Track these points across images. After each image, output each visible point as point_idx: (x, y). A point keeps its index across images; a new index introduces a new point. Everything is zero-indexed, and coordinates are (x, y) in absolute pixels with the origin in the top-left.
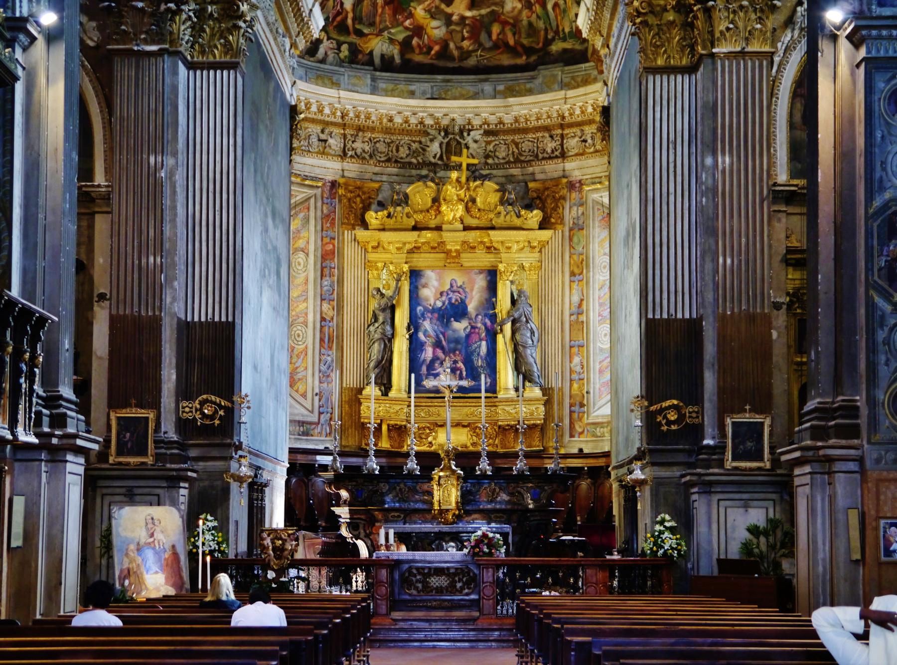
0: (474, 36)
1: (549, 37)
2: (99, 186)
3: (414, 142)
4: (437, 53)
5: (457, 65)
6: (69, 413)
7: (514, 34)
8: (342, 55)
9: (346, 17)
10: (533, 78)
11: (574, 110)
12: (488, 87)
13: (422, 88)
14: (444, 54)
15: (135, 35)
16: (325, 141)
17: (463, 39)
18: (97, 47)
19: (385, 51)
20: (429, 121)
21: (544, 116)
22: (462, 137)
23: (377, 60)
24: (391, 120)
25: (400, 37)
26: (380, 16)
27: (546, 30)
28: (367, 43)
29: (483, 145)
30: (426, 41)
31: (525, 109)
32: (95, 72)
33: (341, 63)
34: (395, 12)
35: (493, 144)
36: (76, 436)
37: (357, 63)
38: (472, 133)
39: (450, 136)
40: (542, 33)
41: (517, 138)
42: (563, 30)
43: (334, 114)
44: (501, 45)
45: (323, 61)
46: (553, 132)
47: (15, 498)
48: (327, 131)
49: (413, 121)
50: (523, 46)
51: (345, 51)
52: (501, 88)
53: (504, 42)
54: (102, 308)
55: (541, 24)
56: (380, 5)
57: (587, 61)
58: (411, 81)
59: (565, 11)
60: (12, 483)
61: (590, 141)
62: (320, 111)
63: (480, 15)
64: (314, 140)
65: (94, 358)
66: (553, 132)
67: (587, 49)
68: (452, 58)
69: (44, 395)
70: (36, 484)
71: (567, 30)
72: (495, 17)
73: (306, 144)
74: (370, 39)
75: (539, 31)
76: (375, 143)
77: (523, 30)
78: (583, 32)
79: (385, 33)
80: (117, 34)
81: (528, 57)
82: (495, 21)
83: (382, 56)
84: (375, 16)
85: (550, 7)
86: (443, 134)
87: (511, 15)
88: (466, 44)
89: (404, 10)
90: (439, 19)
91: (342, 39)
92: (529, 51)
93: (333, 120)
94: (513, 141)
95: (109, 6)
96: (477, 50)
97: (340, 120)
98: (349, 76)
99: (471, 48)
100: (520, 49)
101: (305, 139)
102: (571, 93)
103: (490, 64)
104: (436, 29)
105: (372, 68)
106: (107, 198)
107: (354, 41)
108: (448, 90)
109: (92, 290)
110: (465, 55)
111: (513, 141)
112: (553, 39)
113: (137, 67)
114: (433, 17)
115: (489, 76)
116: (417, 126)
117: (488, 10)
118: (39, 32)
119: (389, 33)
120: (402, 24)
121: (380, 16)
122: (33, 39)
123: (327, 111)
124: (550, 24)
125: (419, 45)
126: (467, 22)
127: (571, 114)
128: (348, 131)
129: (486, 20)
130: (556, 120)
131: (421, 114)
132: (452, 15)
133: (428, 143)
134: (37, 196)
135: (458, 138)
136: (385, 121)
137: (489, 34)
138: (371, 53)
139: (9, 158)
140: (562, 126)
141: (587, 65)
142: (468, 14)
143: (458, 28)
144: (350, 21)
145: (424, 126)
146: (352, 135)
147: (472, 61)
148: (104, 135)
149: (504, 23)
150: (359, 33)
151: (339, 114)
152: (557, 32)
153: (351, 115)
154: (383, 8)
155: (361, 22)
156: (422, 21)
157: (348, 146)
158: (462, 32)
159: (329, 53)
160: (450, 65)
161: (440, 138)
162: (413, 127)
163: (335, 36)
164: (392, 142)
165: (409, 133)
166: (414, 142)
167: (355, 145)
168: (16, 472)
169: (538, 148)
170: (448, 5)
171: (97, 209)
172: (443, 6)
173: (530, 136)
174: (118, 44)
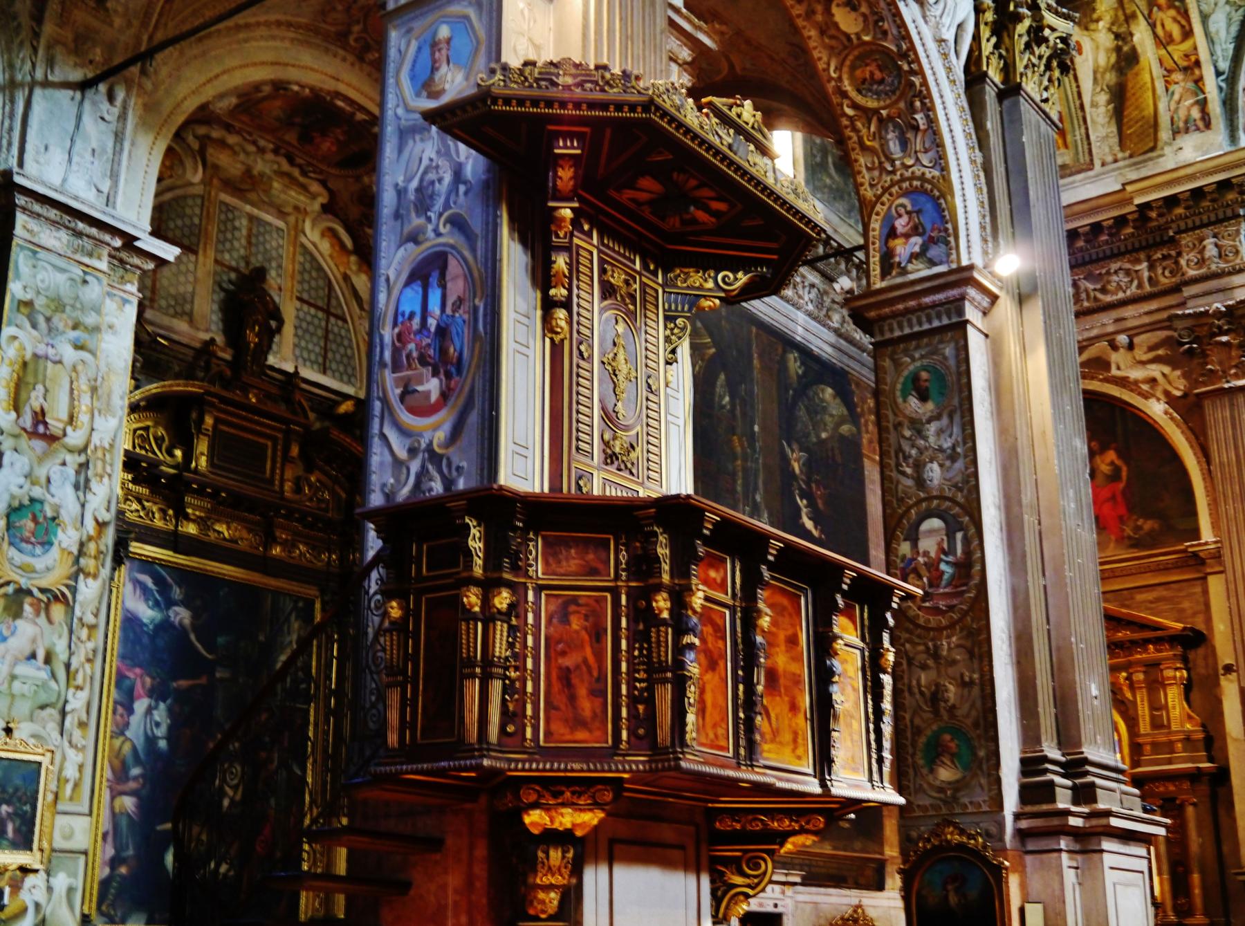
2: (1206, 543)
6: (1098, 781)
15: (1224, 372)
18: (1185, 395)
32: (1186, 422)
36: (1108, 814)
47: (1028, 907)
54: (1231, 681)
60: (1023, 886)
65: (1229, 741)
69: (1063, 759)
70: (1056, 886)
80: (1203, 375)
95: (1191, 348)
106: (1217, 556)
109: (1216, 663)
113: (1232, 405)
118: (1001, 288)
122: (994, 298)
134: (1019, 492)
139: (970, 444)
148: (1206, 487)
168: (1028, 870)
171: (1209, 570)
174: (1206, 386)
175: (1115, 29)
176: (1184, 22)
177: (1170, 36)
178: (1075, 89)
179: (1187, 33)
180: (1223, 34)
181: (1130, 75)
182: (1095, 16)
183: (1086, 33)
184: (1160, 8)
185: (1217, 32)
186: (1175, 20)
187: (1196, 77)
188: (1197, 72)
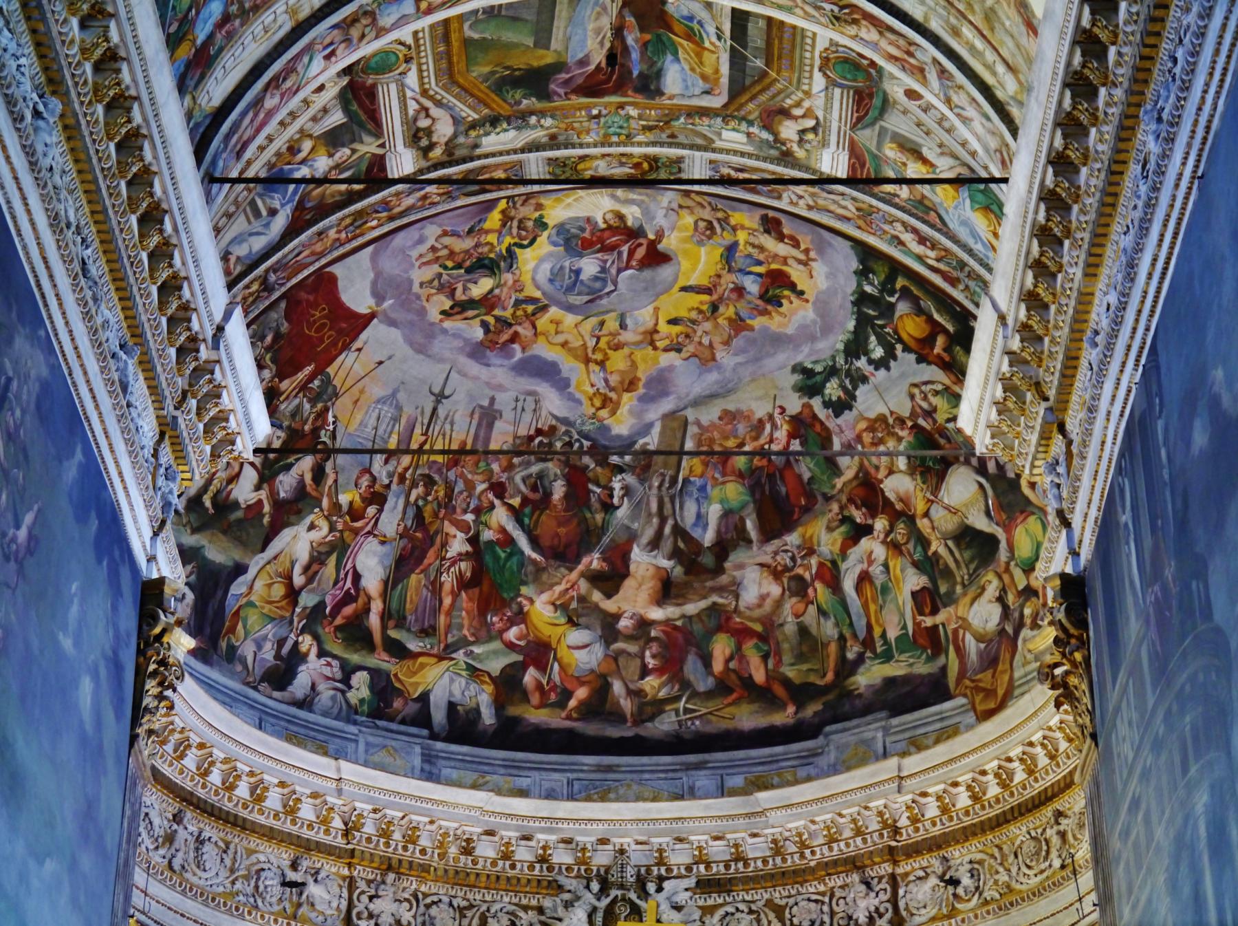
0: (671, 665)
1: (850, 655)
3: (526, 908)
4: (582, 703)
5: (630, 733)
7: (765, 658)
8: (353, 697)
9: (367, 610)
10: (815, 754)
11: (921, 807)
12: (703, 780)
13: (546, 785)
14: (599, 704)
16: (301, 885)
17: (645, 672)
19: (457, 697)
20: (562, 857)
21: (847, 833)
22: (645, 895)
23: (439, 716)
24: (467, 850)
25: (495, 666)
26: (449, 613)
27: (842, 639)
28: (415, 673)
29: (697, 915)
30: (556, 678)
31: (798, 817)
33: (350, 713)
34: (485, 607)
35: (721, 912)
37: (392, 720)
38: (666, 884)
39: (615, 892)
40: (833, 648)
41: (778, 895)
42: (884, 635)
43: (325, 821)
44: (734, 685)
45: (305, 704)
46: (870, 873)
48: (305, 864)
49: (523, 854)
50: (786, 682)
51: (361, 687)
52: (737, 781)
53: (740, 678)
55: (829, 629)
56: (447, 588)
57: (947, 696)
58: (513, 768)
59: (885, 590)
61: (966, 881)
62: (291, 811)
63: (683, 616)
64: (271, 882)
66: (870, 873)
67: (944, 669)
68: (617, 717)
71: (892, 634)
72: (719, 620)
73: (250, 890)
74: (423, 666)
75: (825, 645)
76: (428, 906)
77: (786, 646)
78: (977, 442)
79: (460, 655)
81: (800, 707)
82: (719, 629)
83: (452, 706)
84: (435, 612)
85: (848, 585)
86: (595, 886)
87: (757, 613)
88: (651, 684)
89: (505, 604)
90: (587, 627)
91: (355, 658)
92: (801, 693)
93: (321, 837)
94: (769, 903)
96: (677, 699)
97: (340, 841)
98: (367, 744)
99: (662, 694)
100: (779, 690)
101: (247, 878)
102: (913, 763)
103: (709, 729)
104: (580, 651)
105: (425, 732)
107: (385, 666)
108: (609, 790)
110: (650, 708)
111: (769, 903)
112: (860, 659)
114: (572, 622)
115: (706, 756)
116: (532, 868)
117: (703, 604)
119: (470, 654)
120: (501, 632)
121: (449, 613)
123: (307, 812)
124: (851, 625)
125: (539, 686)
126: (653, 634)
127: (914, 820)
128: (361, 872)
129: (697, 628)
130: (878, 841)
131: (540, 836)
132: (617, 617)
133: (561, 912)
135: (633, 896)
136: (453, 851)
137: (707, 660)
138: (424, 698)
140: (892, 854)
141: (947, 705)
142: (656, 614)
143: (632, 648)
144: (374, 620)
145: (550, 869)
146: (369, 882)
147: (665, 724)
149: (741, 634)
150: (398, 650)
151: (337, 823)
152: (868, 643)
153: (369, 829)
154: (455, 595)
155: (401, 623)
156: (547, 631)
157: (360, 907)
158: (643, 658)
159: (321, 687)
160: (614, 732)
161: (589, 898)
162: (522, 871)
163: (337, 649)
164: (471, 906)
165: (513, 885)
166: (526, 908)
167: (375, 906)
169: (832, 914)
170: (609, 596)
172: (597, 596)
173: (812, 888)
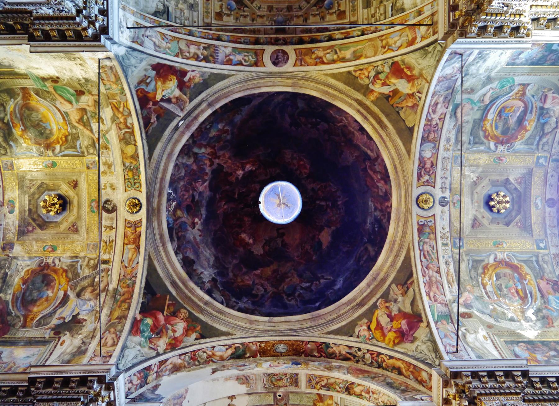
175: (84, 340)
176: (116, 340)
177: (106, 344)
178: (47, 358)
179: (114, 344)
180: (130, 358)
181: (77, 358)
182: (80, 332)
183: (71, 338)
184: (109, 332)
185: (128, 356)
186: (113, 339)
187: (105, 360)
188: (108, 359)
